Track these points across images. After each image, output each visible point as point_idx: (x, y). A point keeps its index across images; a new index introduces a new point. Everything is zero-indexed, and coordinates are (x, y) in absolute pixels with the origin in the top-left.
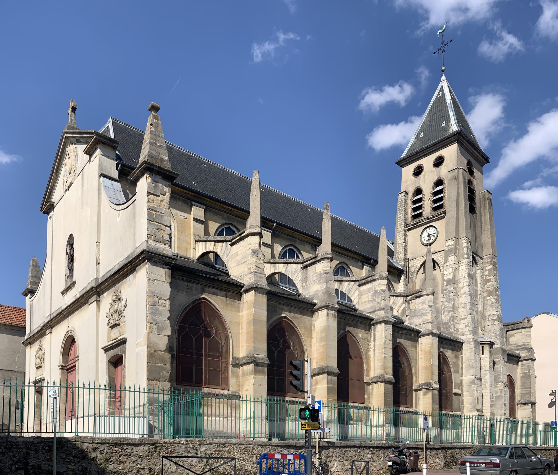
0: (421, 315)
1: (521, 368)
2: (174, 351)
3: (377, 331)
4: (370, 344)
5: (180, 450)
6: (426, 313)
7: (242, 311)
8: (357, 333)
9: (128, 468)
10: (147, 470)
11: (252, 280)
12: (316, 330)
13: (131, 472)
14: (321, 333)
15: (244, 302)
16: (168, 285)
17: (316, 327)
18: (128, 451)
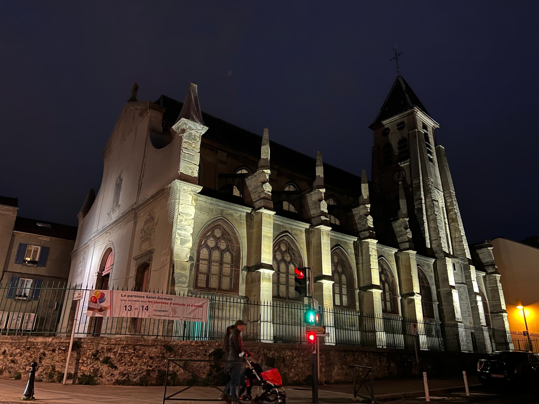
0: (399, 236)
1: (488, 282)
2: (194, 261)
3: (363, 247)
4: (358, 258)
5: (191, 352)
6: (403, 234)
7: (253, 229)
8: (347, 249)
9: (138, 370)
10: (157, 372)
11: (261, 205)
12: (313, 245)
13: (141, 373)
14: (317, 248)
15: (255, 221)
16: (194, 207)
17: (313, 243)
18: (141, 352)
